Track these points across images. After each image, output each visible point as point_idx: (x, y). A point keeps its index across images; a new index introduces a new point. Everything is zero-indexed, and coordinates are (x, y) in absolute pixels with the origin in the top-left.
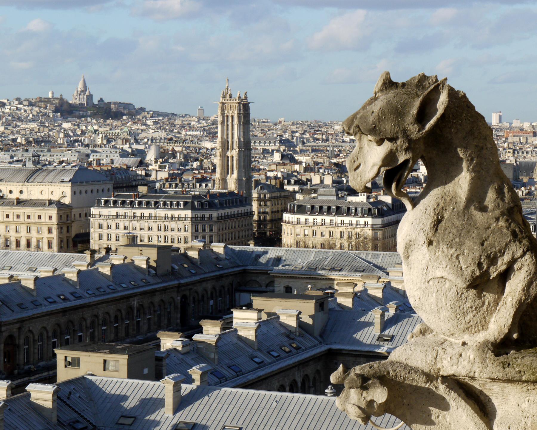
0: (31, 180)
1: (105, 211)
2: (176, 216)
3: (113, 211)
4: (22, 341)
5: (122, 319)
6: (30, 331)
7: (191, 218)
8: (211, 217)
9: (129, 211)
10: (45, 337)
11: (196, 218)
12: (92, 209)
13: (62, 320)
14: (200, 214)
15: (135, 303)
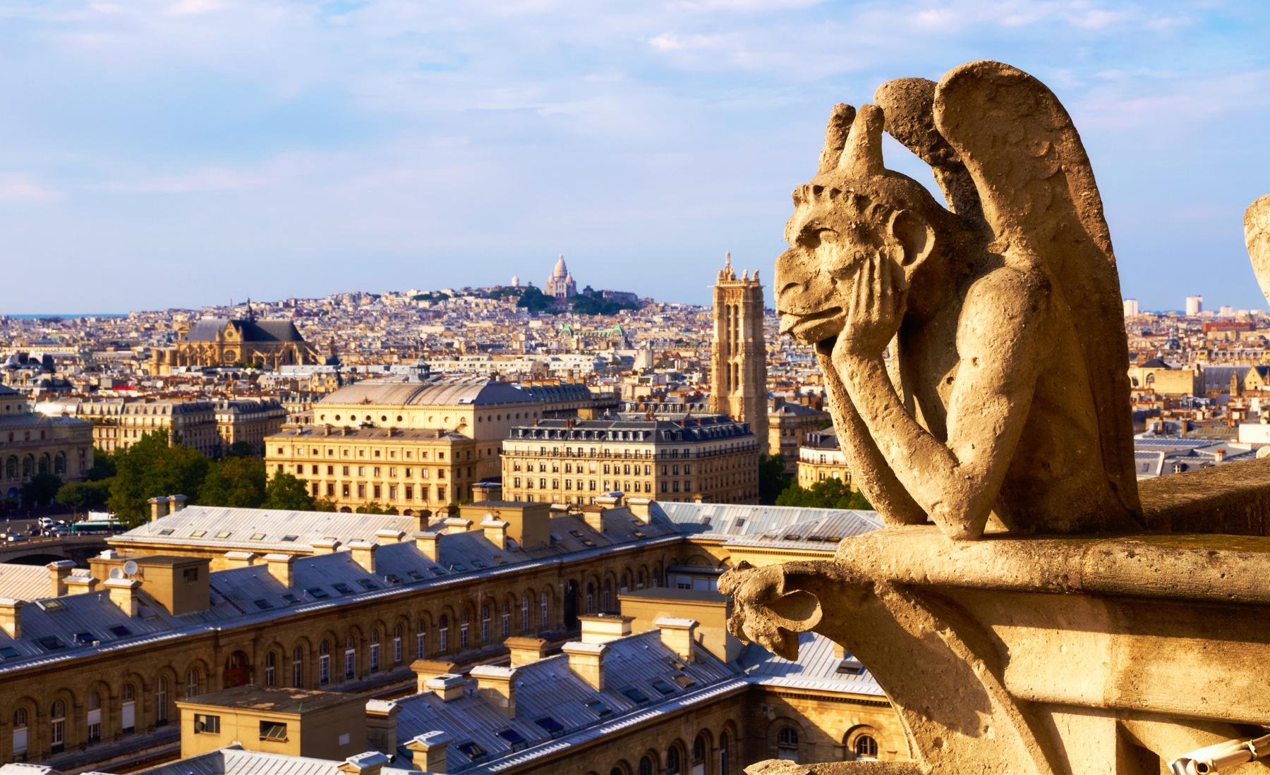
0: (414, 402)
1: (523, 446)
2: (632, 452)
3: (535, 446)
4: (259, 661)
5: (455, 620)
6: (279, 645)
7: (655, 456)
8: (686, 454)
9: (561, 446)
10: (306, 652)
11: (663, 453)
12: (504, 443)
13: (340, 625)
14: (669, 449)
15: (479, 595)
